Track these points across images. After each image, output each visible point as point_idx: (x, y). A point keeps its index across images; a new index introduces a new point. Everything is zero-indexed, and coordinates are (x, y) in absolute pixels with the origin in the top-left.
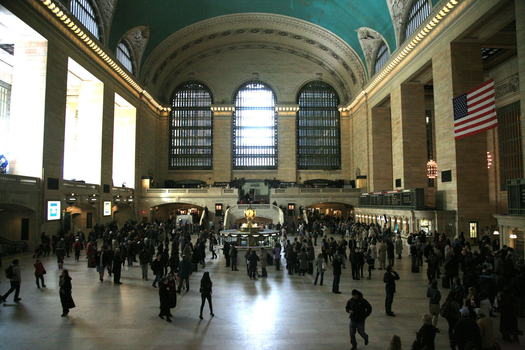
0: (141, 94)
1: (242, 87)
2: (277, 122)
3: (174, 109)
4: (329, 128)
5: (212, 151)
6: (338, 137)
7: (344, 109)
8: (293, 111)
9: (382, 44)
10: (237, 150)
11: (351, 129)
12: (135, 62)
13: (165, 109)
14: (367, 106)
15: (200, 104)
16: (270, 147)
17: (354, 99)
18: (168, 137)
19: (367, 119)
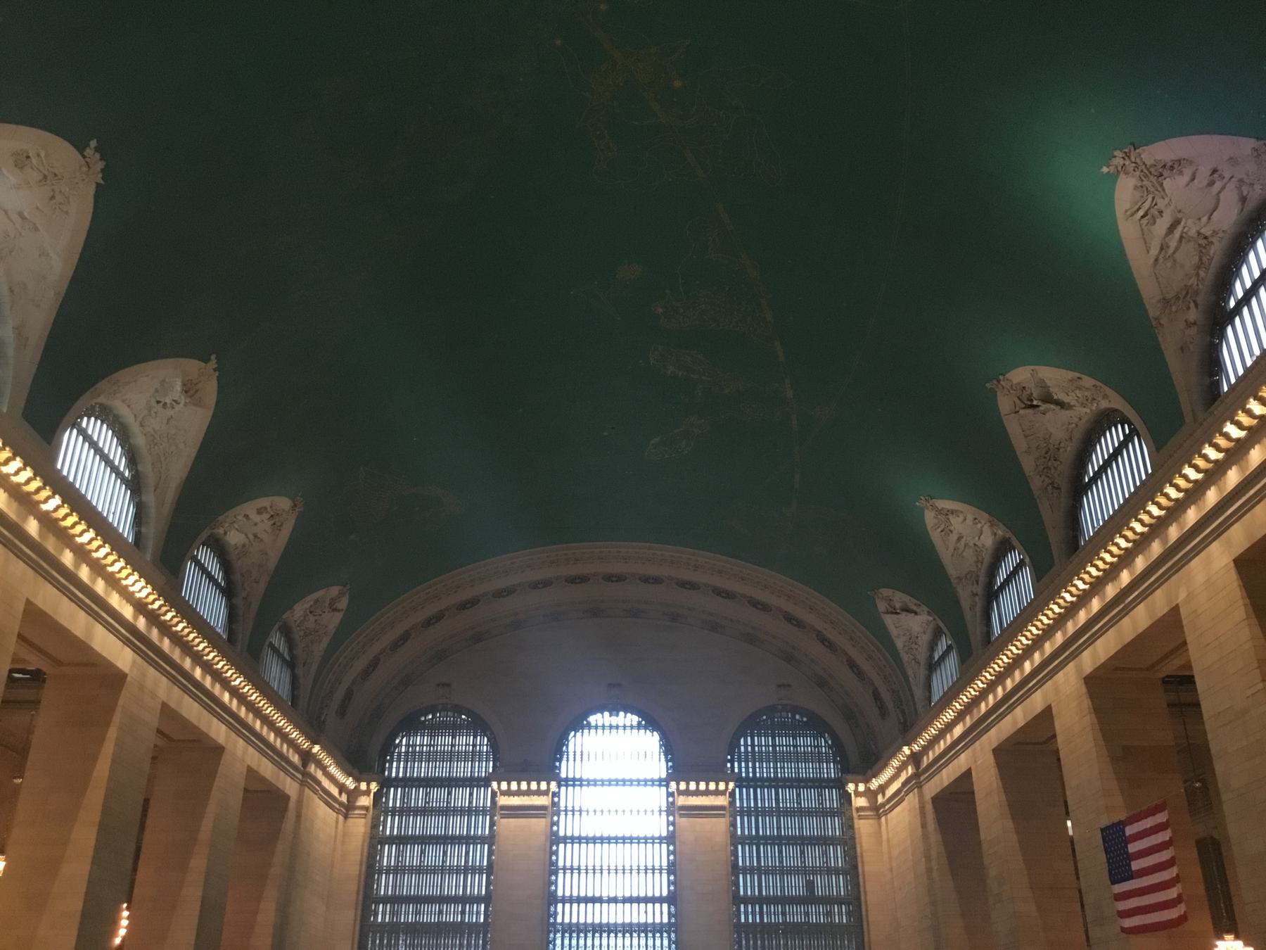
0: (307, 757)
1: (579, 723)
2: (673, 824)
3: (386, 783)
4: (824, 841)
6: (852, 869)
7: (861, 787)
8: (717, 793)
9: (937, 634)
10: (560, 906)
11: (885, 847)
12: (300, 671)
13: (363, 786)
14: (920, 786)
15: (462, 769)
16: (653, 900)
17: (885, 765)
18: (364, 869)
19: (924, 826)
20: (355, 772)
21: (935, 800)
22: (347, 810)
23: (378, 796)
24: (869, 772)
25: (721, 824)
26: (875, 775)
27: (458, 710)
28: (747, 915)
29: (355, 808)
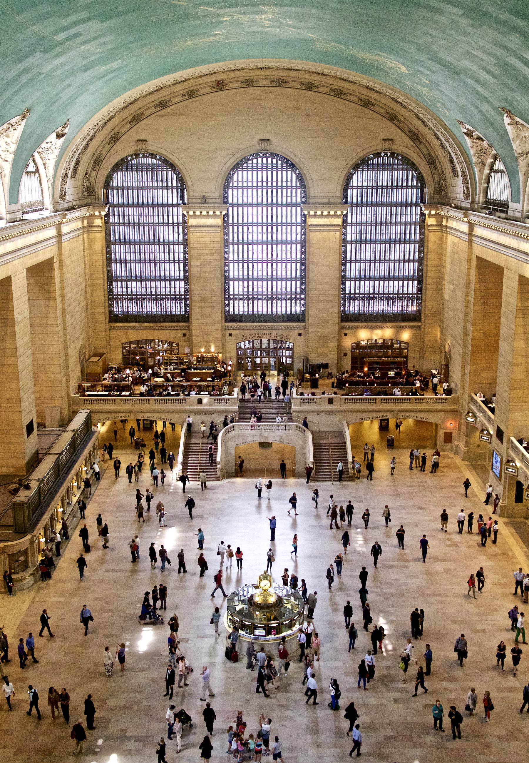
7: (433, 212)
8: (335, 216)
27: (152, 156)
28: (351, 287)
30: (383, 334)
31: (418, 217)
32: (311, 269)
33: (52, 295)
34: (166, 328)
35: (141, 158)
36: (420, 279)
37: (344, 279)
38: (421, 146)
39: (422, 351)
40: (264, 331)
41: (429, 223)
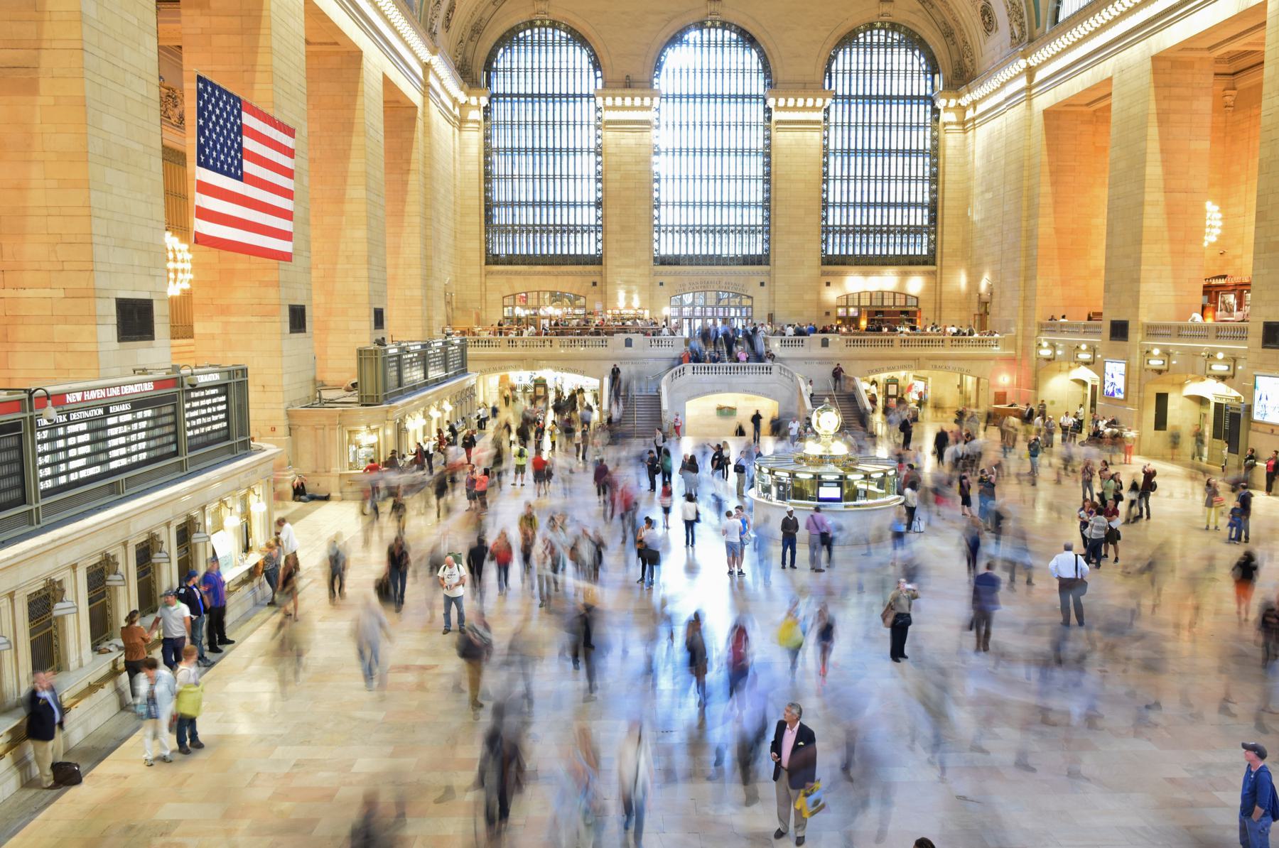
0: (427, 67)
3: (493, 97)
5: (597, 218)
6: (934, 178)
7: (953, 103)
8: (814, 108)
13: (473, 100)
14: (1030, 98)
20: (466, 86)
21: (1047, 113)
22: (461, 122)
23: (487, 110)
24: (964, 88)
25: (815, 137)
26: (969, 92)
27: (554, 25)
28: (835, 217)
29: (467, 122)
30: (885, 281)
31: (928, 115)
32: (778, 185)
33: (413, 166)
34: (568, 274)
35: (539, 27)
36: (933, 208)
37: (825, 205)
38: (933, 11)
39: (938, 307)
40: (710, 278)
41: (946, 120)
